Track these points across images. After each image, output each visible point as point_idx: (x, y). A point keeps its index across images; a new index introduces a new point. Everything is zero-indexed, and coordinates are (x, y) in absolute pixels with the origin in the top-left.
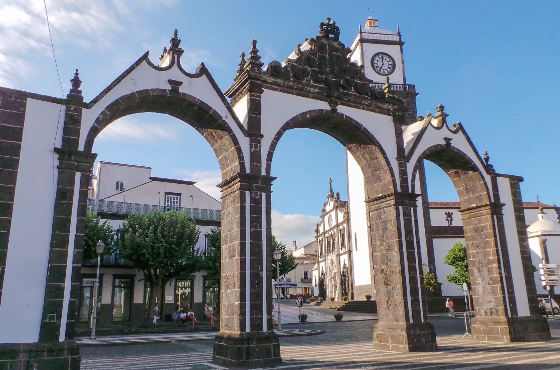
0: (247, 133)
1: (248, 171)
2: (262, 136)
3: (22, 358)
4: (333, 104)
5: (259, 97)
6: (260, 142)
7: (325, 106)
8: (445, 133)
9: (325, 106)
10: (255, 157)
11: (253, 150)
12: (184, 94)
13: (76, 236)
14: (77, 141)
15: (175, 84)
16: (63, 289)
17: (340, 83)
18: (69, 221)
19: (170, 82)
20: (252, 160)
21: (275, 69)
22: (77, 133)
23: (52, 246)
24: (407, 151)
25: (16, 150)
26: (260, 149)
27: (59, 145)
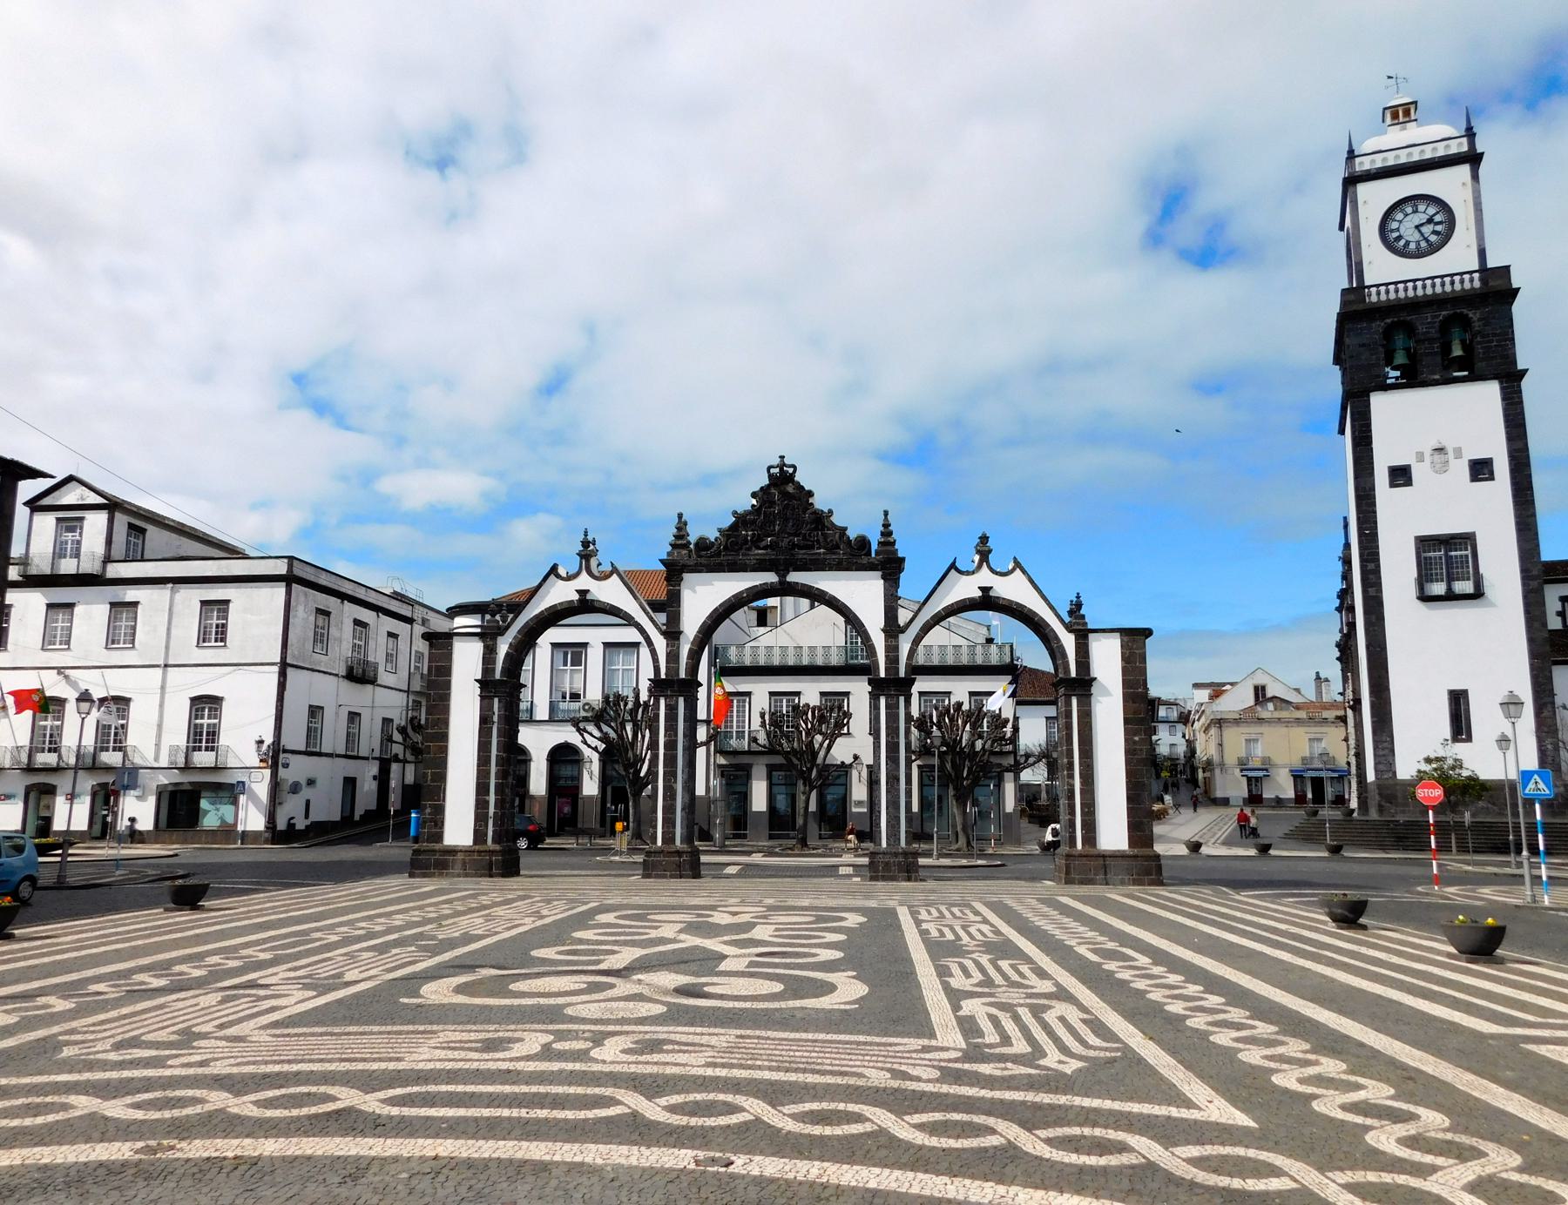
0: (664, 634)
1: (663, 676)
2: (681, 632)
3: (460, 856)
4: (782, 574)
5: (680, 585)
6: (678, 639)
7: (770, 578)
8: (985, 577)
9: (770, 578)
10: (673, 657)
11: (669, 649)
12: (593, 601)
13: (497, 756)
14: (494, 669)
15: (583, 593)
16: (488, 802)
17: (794, 542)
18: (490, 743)
19: (578, 591)
20: (667, 662)
21: (703, 544)
22: (494, 663)
23: (478, 766)
24: (902, 621)
25: (448, 685)
26: (679, 647)
27: (479, 677)
